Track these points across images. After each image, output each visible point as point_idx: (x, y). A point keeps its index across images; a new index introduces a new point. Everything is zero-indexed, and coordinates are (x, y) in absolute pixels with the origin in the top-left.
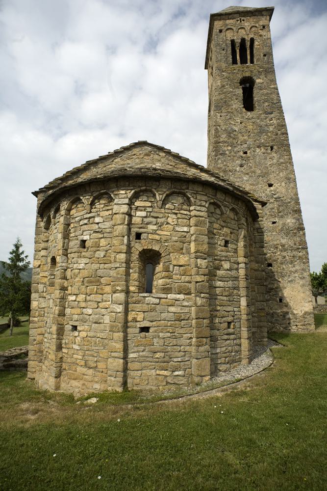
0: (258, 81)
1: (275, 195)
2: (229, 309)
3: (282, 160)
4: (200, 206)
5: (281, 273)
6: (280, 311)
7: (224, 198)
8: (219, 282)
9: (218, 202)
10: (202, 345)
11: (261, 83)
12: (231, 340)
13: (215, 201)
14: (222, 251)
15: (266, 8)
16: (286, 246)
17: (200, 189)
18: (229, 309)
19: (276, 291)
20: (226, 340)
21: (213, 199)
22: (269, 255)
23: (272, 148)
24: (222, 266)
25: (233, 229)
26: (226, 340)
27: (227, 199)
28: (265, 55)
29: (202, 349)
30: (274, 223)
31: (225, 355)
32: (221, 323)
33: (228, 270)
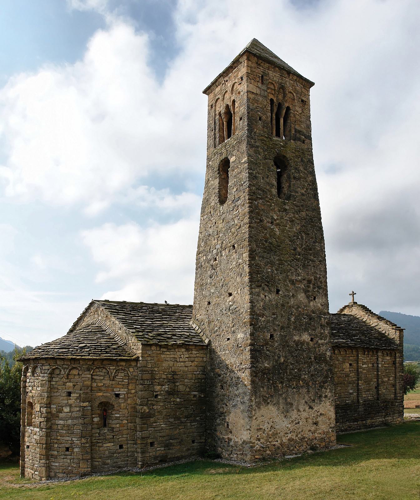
0: (232, 159)
1: (232, 305)
2: (68, 438)
3: (240, 261)
4: (44, 373)
5: (229, 396)
6: (227, 437)
7: (63, 363)
8: (61, 421)
9: (59, 367)
10: (42, 460)
11: (235, 161)
12: (68, 459)
13: (57, 366)
14: (63, 400)
15: (240, 55)
16: (234, 366)
17: (45, 362)
18: (68, 438)
19: (225, 416)
20: (64, 459)
21: (55, 366)
22: (222, 376)
23: (234, 246)
24: (63, 410)
25: (77, 382)
26: (64, 459)
27: (65, 363)
28: (241, 119)
29: (41, 461)
30: (228, 339)
31: (62, 468)
32: (59, 447)
33: (67, 412)
